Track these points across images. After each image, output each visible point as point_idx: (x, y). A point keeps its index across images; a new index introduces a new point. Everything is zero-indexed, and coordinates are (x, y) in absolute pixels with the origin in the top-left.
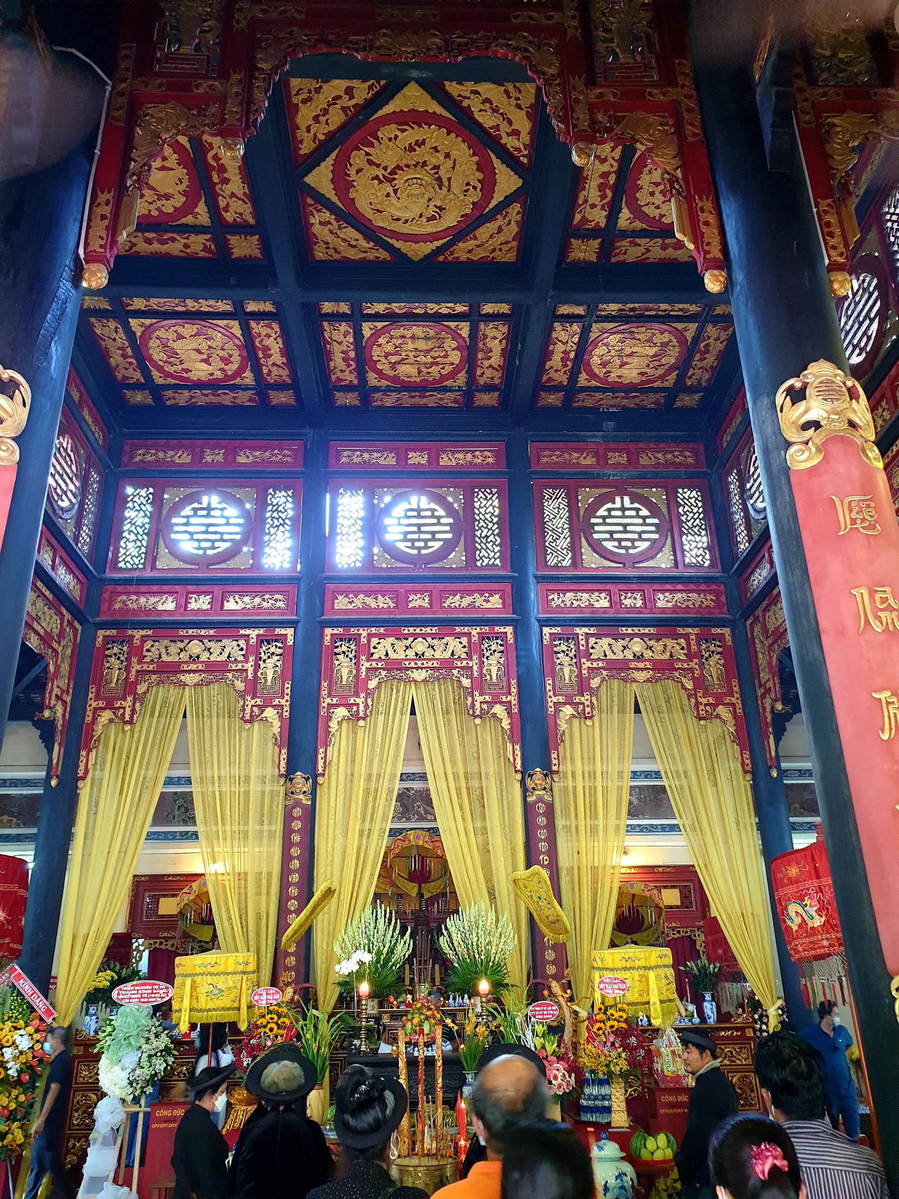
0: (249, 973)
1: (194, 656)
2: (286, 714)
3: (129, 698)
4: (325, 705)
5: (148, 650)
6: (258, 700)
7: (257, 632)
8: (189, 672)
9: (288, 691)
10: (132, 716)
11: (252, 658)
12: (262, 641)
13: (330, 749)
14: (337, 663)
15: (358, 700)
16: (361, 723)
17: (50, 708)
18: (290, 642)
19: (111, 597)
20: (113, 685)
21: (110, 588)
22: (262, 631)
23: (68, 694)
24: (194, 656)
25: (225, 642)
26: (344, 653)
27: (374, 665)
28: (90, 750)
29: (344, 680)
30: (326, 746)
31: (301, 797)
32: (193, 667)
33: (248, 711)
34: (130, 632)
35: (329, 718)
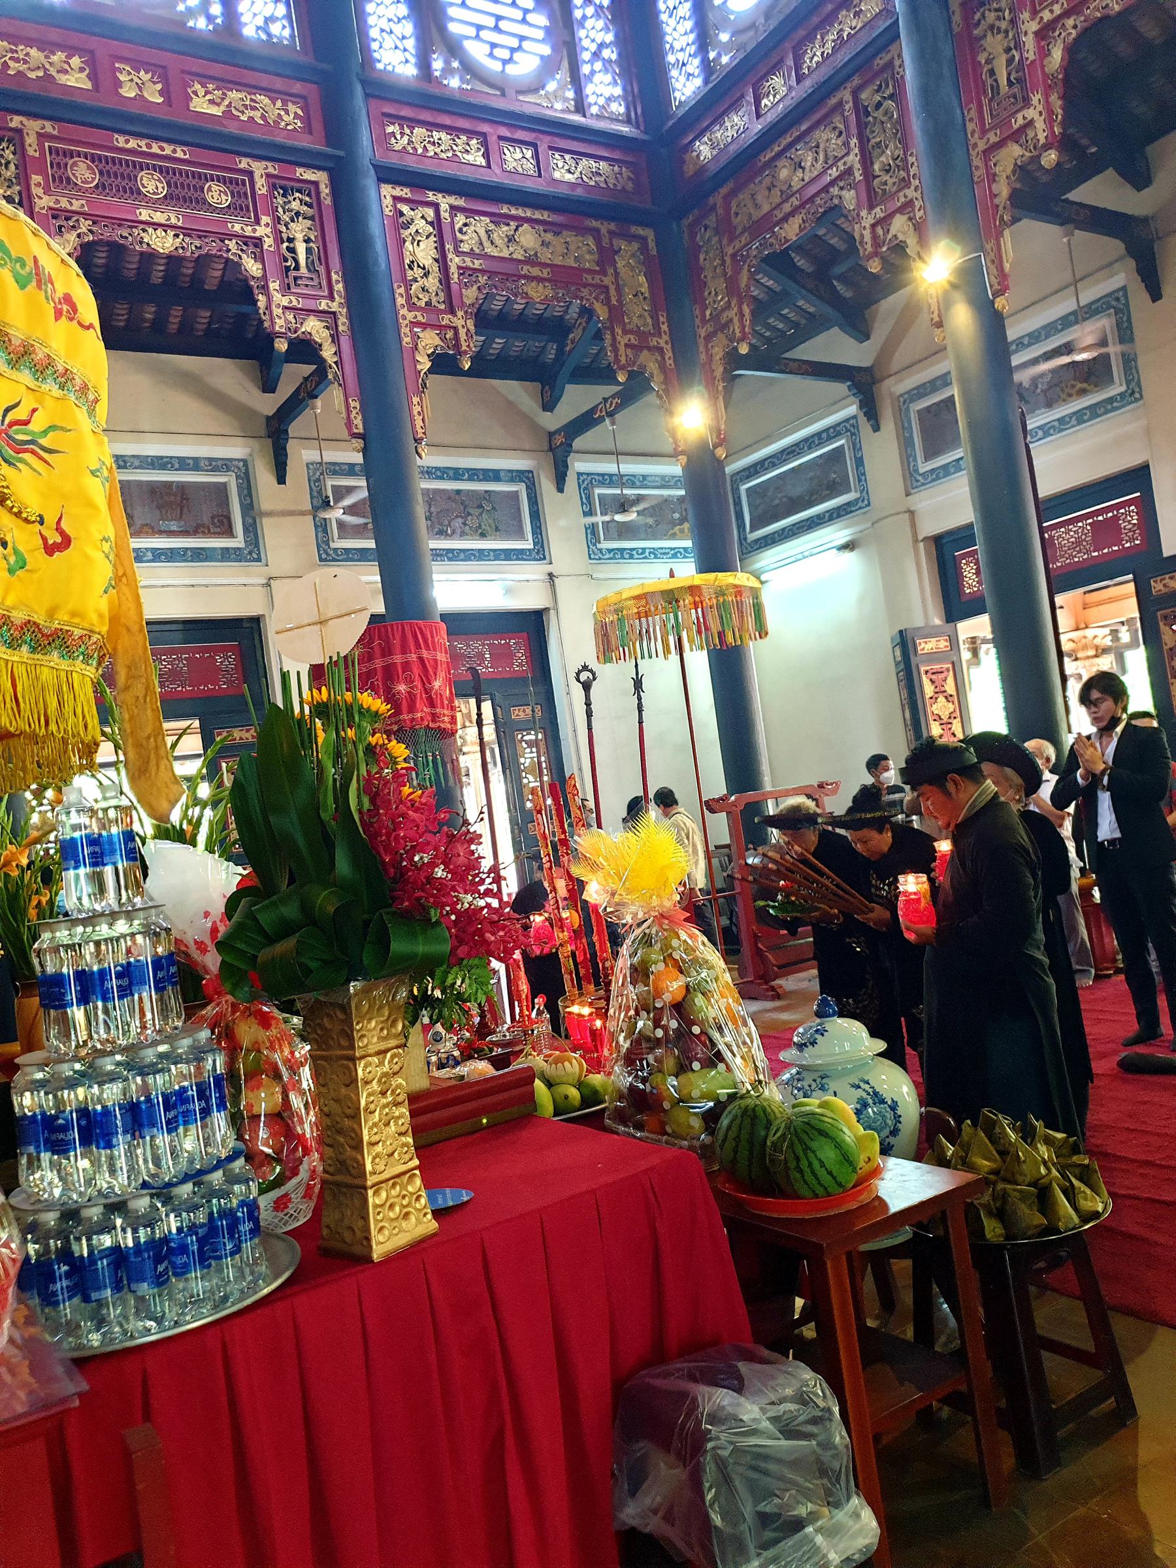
6: (878, 210)
8: (785, 219)
15: (1030, 113)
17: (622, 368)
26: (992, 27)
32: (787, 208)
34: (711, 200)
35: (992, 178)
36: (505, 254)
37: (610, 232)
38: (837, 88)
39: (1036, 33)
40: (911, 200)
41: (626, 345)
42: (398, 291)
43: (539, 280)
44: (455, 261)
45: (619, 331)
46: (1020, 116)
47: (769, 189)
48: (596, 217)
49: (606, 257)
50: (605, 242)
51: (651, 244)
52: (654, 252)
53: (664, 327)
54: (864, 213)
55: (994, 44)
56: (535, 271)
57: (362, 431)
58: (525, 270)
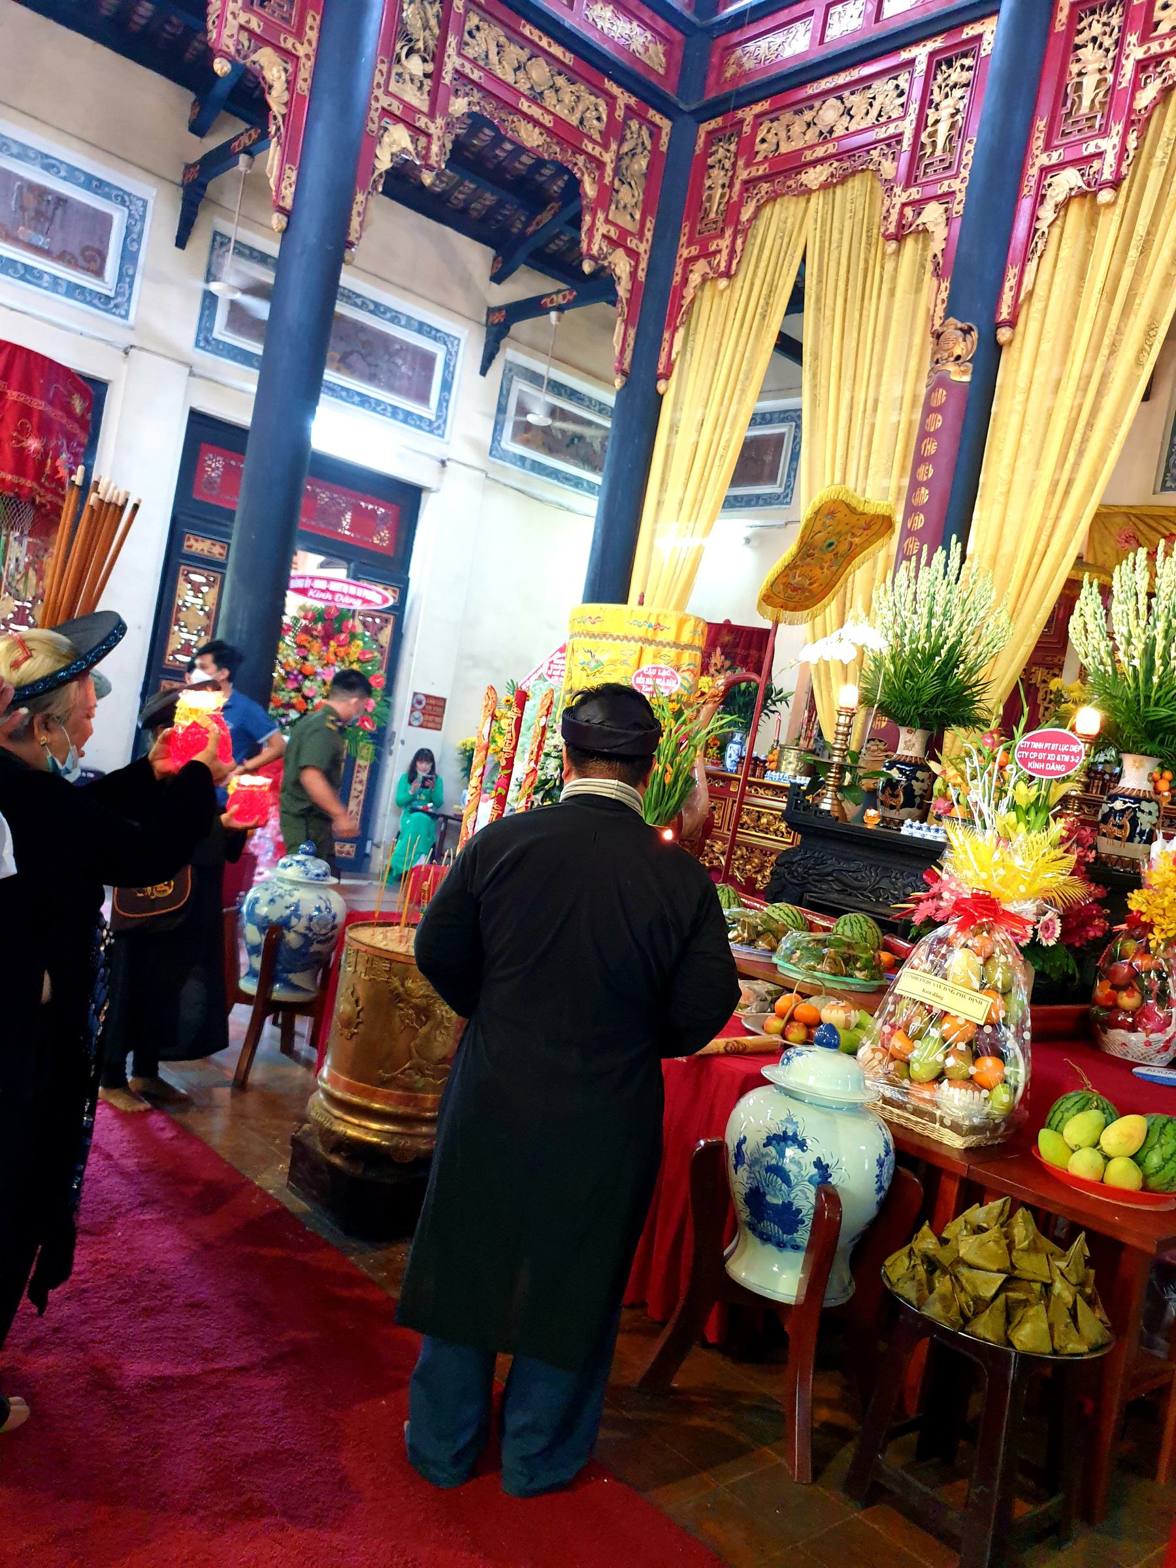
0: (660, 643)
1: (825, 130)
2: (958, 208)
3: (729, 232)
4: (1034, 171)
5: (763, 141)
6: (913, 190)
7: (931, 46)
8: (814, 163)
9: (968, 159)
10: (729, 266)
11: (914, 108)
12: (939, 64)
13: (1031, 267)
14: (1075, 68)
16: (1105, 196)
17: (592, 257)
18: (987, 47)
19: (722, 58)
20: (712, 215)
21: (722, 42)
22: (937, 43)
23: (641, 239)
24: (825, 130)
25: (877, 85)
26: (1094, 40)
27: (1155, 48)
28: (676, 329)
29: (1086, 103)
30: (1025, 260)
31: (951, 367)
32: (820, 152)
33: (894, 217)
34: (740, 114)
35: (1040, 199)
36: (510, 79)
37: (628, 107)
38: (916, 42)
39: (1138, 62)
40: (954, 192)
41: (604, 236)
42: (380, 66)
43: (537, 123)
44: (452, 61)
45: (601, 215)
46: (1092, 144)
47: (809, 125)
48: (620, 84)
49: (614, 131)
50: (620, 113)
51: (665, 139)
52: (664, 149)
53: (649, 235)
54: (898, 190)
55: (1091, 58)
56: (535, 112)
57: (288, 203)
58: (524, 105)
